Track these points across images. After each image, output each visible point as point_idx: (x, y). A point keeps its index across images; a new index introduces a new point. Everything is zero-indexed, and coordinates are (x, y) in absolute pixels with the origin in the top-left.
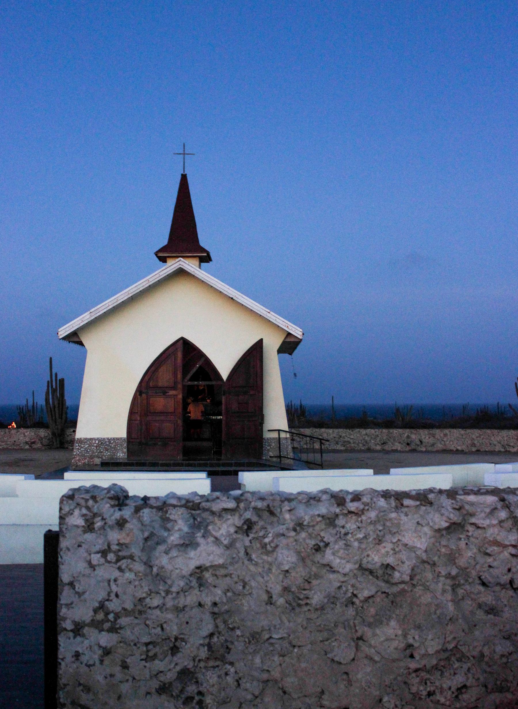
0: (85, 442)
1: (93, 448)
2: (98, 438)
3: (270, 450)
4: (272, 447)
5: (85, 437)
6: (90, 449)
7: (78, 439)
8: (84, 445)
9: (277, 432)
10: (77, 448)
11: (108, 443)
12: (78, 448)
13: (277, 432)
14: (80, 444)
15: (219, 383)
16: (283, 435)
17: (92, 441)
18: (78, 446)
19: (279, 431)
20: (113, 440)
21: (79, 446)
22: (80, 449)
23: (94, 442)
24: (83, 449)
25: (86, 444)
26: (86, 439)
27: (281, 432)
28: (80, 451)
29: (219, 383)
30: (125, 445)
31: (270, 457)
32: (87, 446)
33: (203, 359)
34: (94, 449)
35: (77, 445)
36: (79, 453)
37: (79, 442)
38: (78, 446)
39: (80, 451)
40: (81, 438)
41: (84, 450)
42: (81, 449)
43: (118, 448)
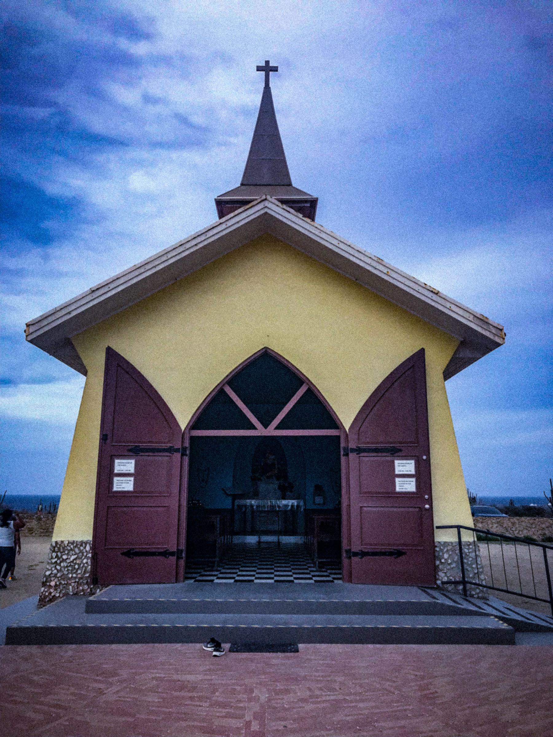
0: (71, 550)
1: (85, 561)
3: (440, 567)
4: (443, 561)
6: (79, 565)
8: (68, 554)
9: (456, 529)
10: (54, 561)
12: (56, 562)
13: (456, 529)
14: (59, 554)
17: (85, 547)
18: (57, 556)
19: (459, 527)
21: (59, 559)
24: (65, 564)
25: (71, 553)
26: (73, 543)
28: (58, 567)
31: (443, 583)
32: (73, 557)
34: (87, 563)
36: (55, 571)
37: (59, 549)
38: (57, 556)
39: (58, 567)
40: (62, 542)
41: (67, 567)
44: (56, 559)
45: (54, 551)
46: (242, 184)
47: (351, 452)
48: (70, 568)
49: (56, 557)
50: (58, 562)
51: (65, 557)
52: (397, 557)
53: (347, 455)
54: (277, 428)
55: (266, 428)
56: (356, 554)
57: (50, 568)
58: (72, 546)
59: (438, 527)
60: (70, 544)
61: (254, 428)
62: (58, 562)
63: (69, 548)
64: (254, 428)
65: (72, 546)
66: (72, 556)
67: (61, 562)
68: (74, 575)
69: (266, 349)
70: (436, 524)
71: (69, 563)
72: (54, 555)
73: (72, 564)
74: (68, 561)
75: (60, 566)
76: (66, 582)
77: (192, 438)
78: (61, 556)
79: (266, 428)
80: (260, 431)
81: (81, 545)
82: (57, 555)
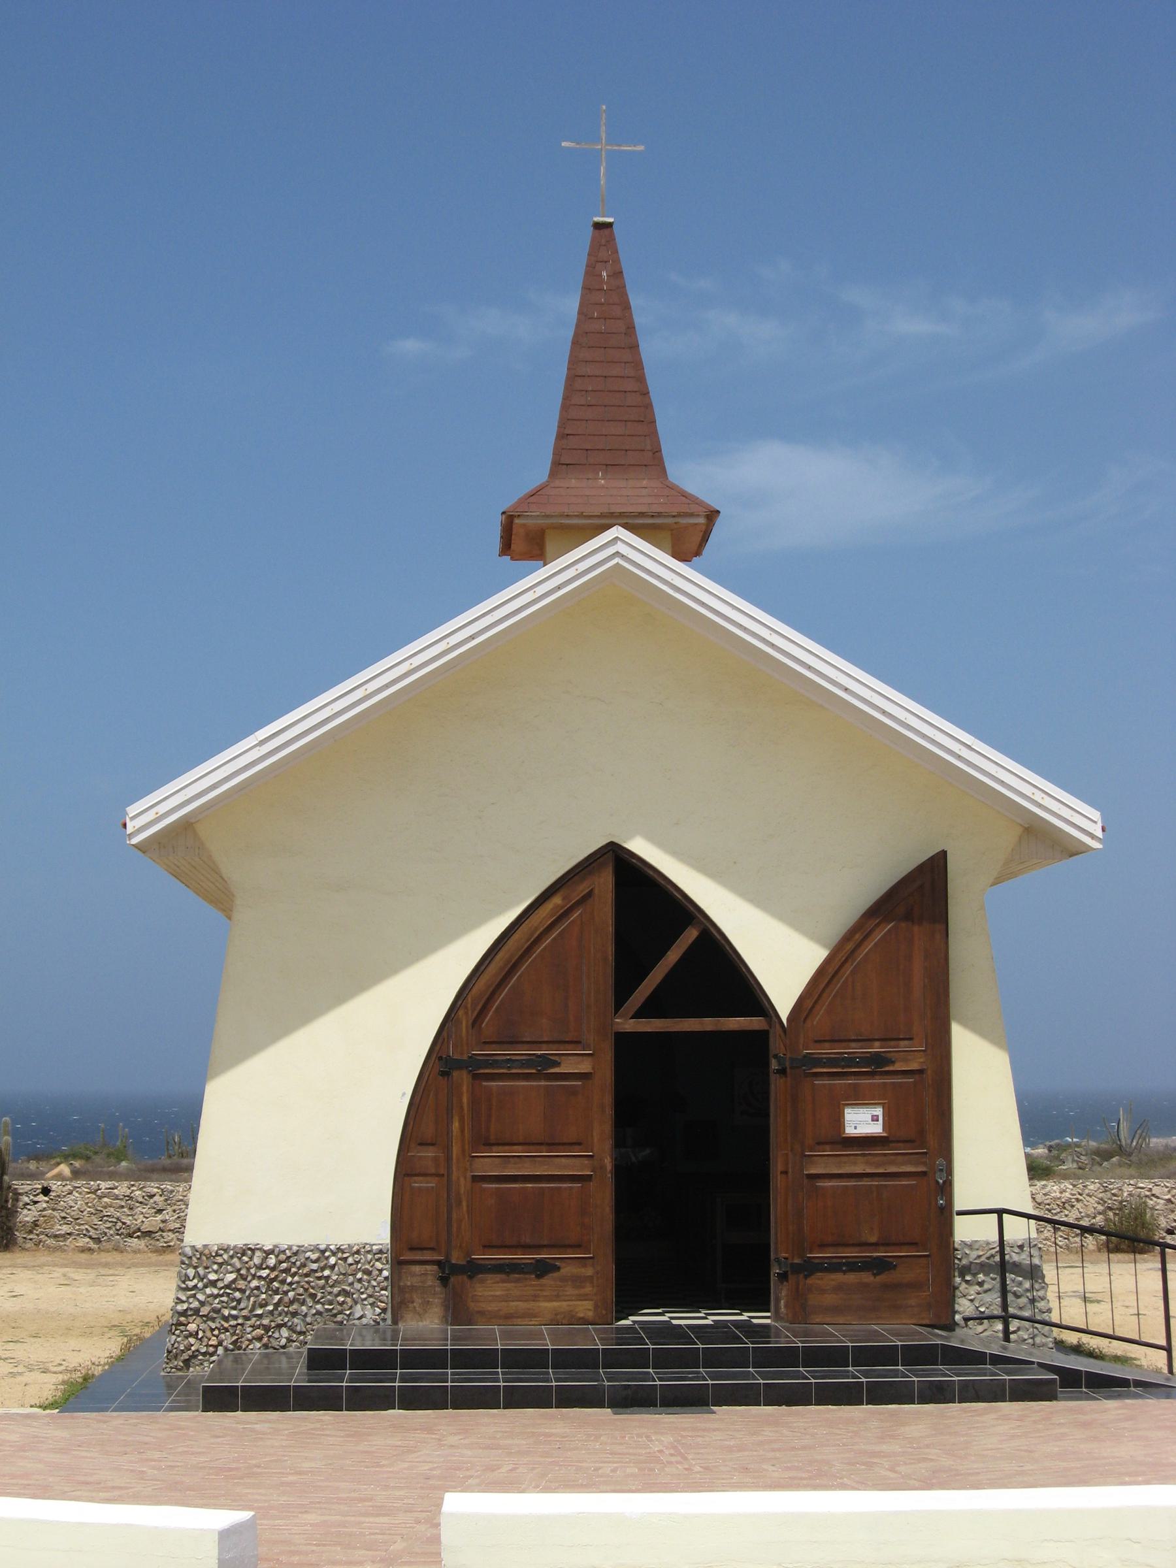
0: (225, 1263)
2: (276, 1246)
9: (996, 1215)
11: (314, 1266)
12: (195, 1287)
13: (996, 1215)
14: (201, 1271)
16: (1017, 1230)
17: (251, 1258)
18: (197, 1275)
19: (1000, 1212)
20: (334, 1254)
23: (257, 1260)
24: (216, 1291)
27: (1005, 1216)
30: (386, 1273)
32: (231, 1277)
40: (205, 1246)
42: (208, 1291)
43: (357, 1286)
44: (195, 1281)
45: (189, 1266)
46: (559, 466)
48: (225, 1299)
50: (200, 1285)
51: (212, 1277)
54: (638, 1015)
57: (184, 1298)
59: (960, 1213)
62: (200, 1285)
66: (228, 1275)
67: (206, 1286)
68: (234, 1312)
70: (958, 1205)
71: (221, 1289)
72: (191, 1272)
73: (228, 1291)
74: (220, 1284)
75: (205, 1293)
76: (218, 1325)
81: (244, 1254)
82: (197, 1273)
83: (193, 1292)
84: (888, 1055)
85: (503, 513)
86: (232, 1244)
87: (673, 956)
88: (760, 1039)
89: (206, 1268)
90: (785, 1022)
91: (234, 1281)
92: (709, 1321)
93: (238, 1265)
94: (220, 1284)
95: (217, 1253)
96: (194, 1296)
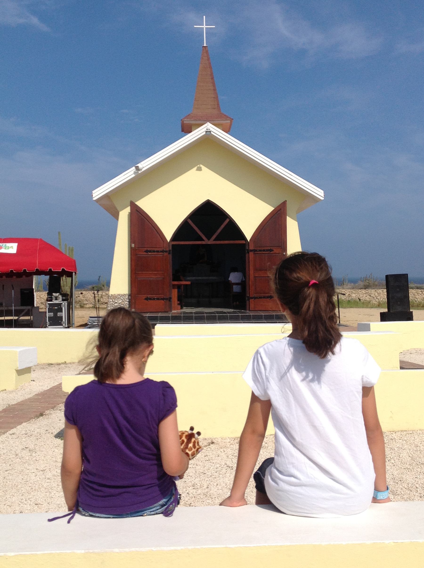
0: (119, 298)
5: (119, 293)
7: (112, 295)
10: (111, 303)
12: (112, 304)
14: (114, 300)
15: (243, 242)
17: (125, 297)
22: (114, 305)
24: (117, 305)
26: (119, 295)
29: (243, 242)
33: (228, 220)
35: (111, 300)
40: (114, 294)
42: (115, 305)
44: (112, 302)
47: (250, 252)
49: (112, 301)
50: (113, 303)
51: (116, 301)
52: (270, 299)
53: (249, 253)
55: (209, 240)
56: (252, 298)
58: (119, 297)
60: (118, 296)
61: (202, 240)
62: (113, 303)
63: (118, 297)
64: (202, 240)
65: (119, 297)
67: (115, 303)
69: (208, 200)
73: (120, 304)
74: (118, 303)
77: (173, 245)
78: (115, 301)
79: (209, 240)
80: (206, 242)
82: (113, 301)
83: (112, 305)
84: (273, 249)
85: (181, 120)
86: (121, 294)
87: (223, 226)
88: (244, 245)
89: (115, 299)
90: (249, 241)
91: (121, 302)
92: (232, 311)
93: (122, 299)
94: (118, 303)
95: (117, 295)
96: (112, 306)
